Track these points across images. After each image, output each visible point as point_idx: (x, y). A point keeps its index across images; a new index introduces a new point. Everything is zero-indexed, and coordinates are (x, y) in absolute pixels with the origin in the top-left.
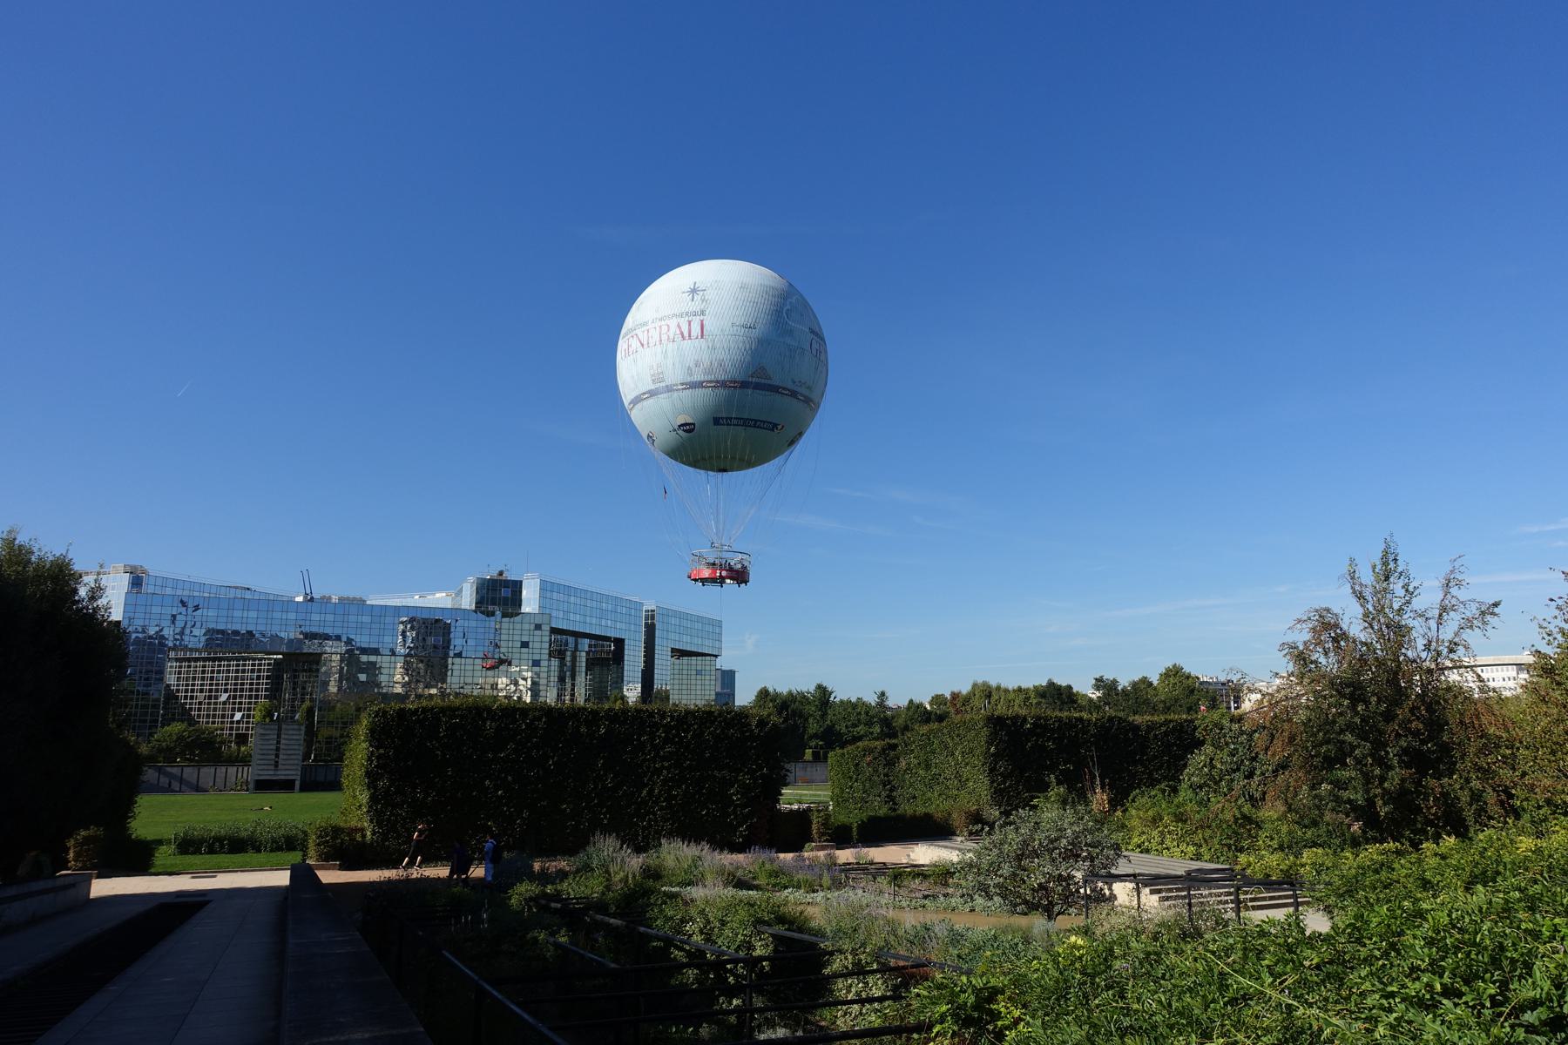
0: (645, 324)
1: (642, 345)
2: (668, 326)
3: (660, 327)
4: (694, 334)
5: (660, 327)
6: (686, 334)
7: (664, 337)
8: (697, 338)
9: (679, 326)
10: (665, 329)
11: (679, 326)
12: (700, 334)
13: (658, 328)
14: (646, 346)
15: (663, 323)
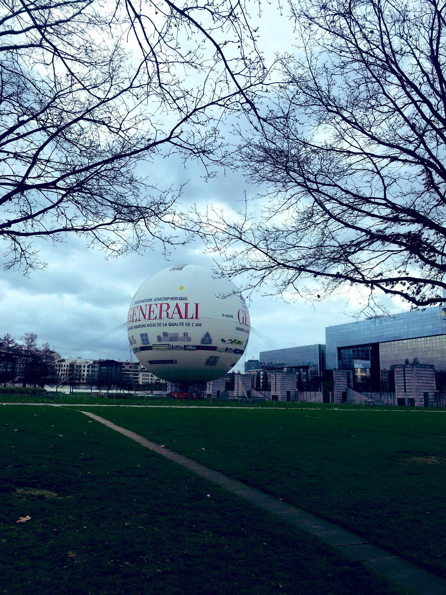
0: (150, 300)
1: (144, 316)
2: (168, 305)
3: (161, 305)
4: (190, 315)
5: (161, 305)
6: (183, 315)
7: (164, 314)
8: (192, 318)
9: (177, 305)
10: (165, 307)
11: (177, 305)
12: (195, 316)
13: (159, 306)
14: (147, 316)
15: (165, 302)
